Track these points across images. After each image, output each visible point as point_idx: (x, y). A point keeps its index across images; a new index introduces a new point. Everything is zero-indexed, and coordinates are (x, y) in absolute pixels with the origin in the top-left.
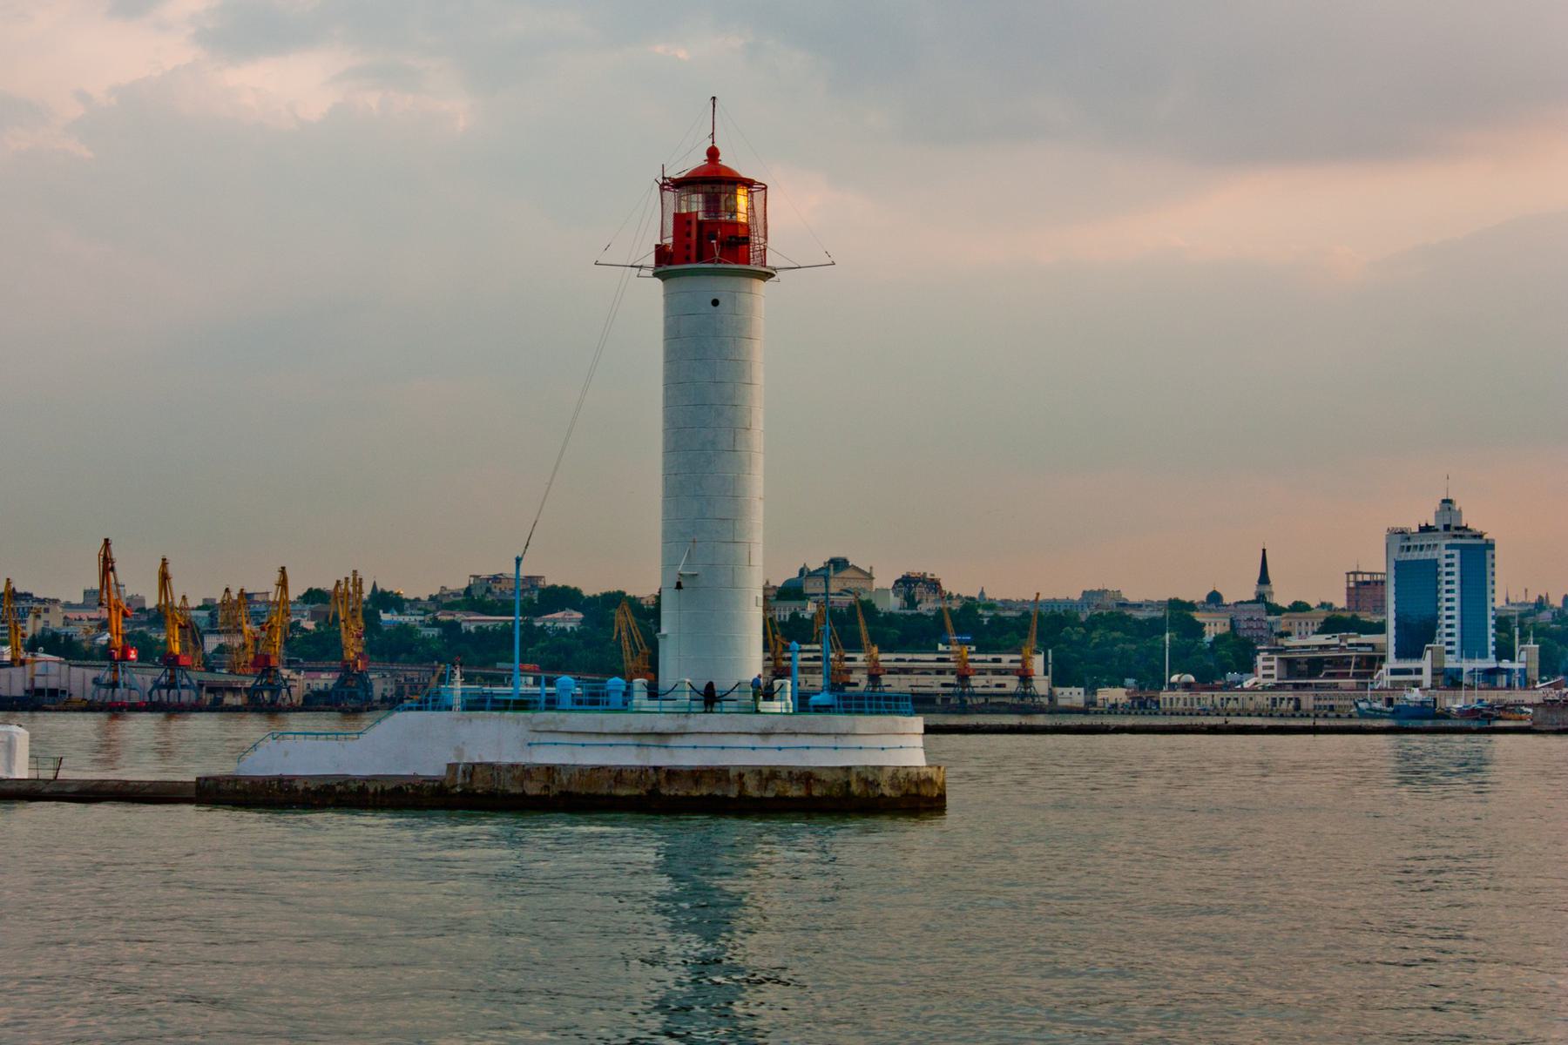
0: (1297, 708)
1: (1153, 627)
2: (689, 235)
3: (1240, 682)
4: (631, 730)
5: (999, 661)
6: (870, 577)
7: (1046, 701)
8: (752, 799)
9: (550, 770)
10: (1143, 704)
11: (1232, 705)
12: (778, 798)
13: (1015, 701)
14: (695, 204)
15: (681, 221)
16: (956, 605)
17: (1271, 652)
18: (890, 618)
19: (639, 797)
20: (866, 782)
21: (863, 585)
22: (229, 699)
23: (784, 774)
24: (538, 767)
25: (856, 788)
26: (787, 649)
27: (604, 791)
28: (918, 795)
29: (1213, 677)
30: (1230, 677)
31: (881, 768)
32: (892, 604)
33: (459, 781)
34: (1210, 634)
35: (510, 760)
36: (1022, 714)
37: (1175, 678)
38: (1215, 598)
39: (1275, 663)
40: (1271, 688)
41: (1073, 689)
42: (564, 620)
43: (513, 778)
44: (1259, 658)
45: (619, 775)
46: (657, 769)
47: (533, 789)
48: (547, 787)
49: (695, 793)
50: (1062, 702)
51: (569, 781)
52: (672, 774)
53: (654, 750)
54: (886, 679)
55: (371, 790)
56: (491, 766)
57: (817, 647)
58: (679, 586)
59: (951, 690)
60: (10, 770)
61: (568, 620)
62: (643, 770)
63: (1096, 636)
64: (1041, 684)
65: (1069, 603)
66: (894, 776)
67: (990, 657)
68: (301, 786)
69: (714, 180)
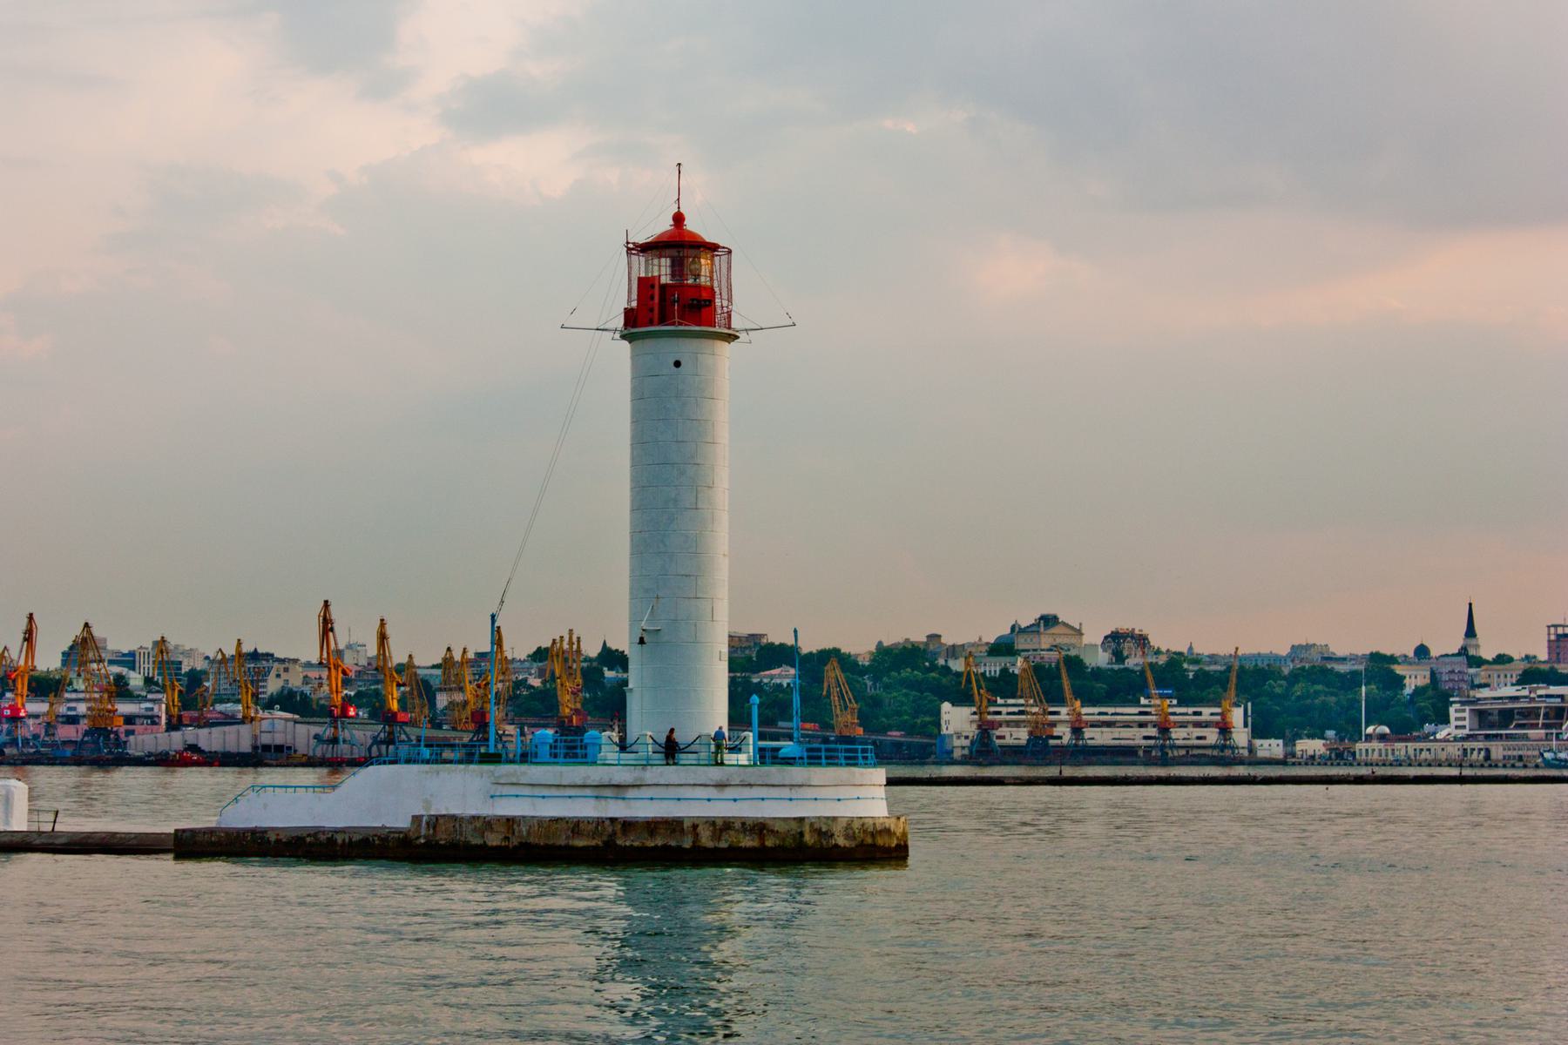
0: (1487, 758)
1: (1352, 680)
2: (652, 298)
3: (1434, 734)
4: (589, 782)
5: (1200, 714)
6: (1079, 633)
7: (1245, 753)
8: (706, 849)
9: (510, 821)
10: (1340, 755)
11: (1425, 755)
12: (731, 848)
13: (1215, 753)
14: (662, 270)
15: (646, 285)
16: (1162, 660)
17: (1462, 703)
18: (1097, 673)
19: (596, 847)
20: (819, 832)
21: (1073, 640)
22: (447, 754)
23: (738, 825)
24: (499, 819)
25: (809, 839)
26: (994, 703)
27: (562, 842)
28: (874, 845)
29: (1411, 730)
30: (1428, 727)
31: (834, 819)
32: (1101, 659)
33: (423, 832)
34: (1409, 687)
35: (473, 812)
36: (1223, 766)
37: (1370, 730)
38: (1422, 651)
39: (1466, 714)
40: (1463, 739)
41: (1273, 742)
42: (780, 676)
43: (475, 829)
44: (1452, 710)
45: (576, 826)
46: (613, 820)
47: (494, 840)
48: (506, 838)
49: (650, 844)
50: (1261, 754)
51: (529, 833)
52: (628, 825)
53: (611, 802)
54: (1088, 733)
55: (340, 841)
56: (454, 818)
57: (1022, 701)
58: (642, 641)
59: (1152, 742)
60: (7, 823)
61: (784, 676)
62: (600, 822)
63: (1298, 689)
64: (1241, 736)
65: (1277, 658)
66: (849, 826)
67: (1191, 710)
68: (273, 838)
69: (679, 245)
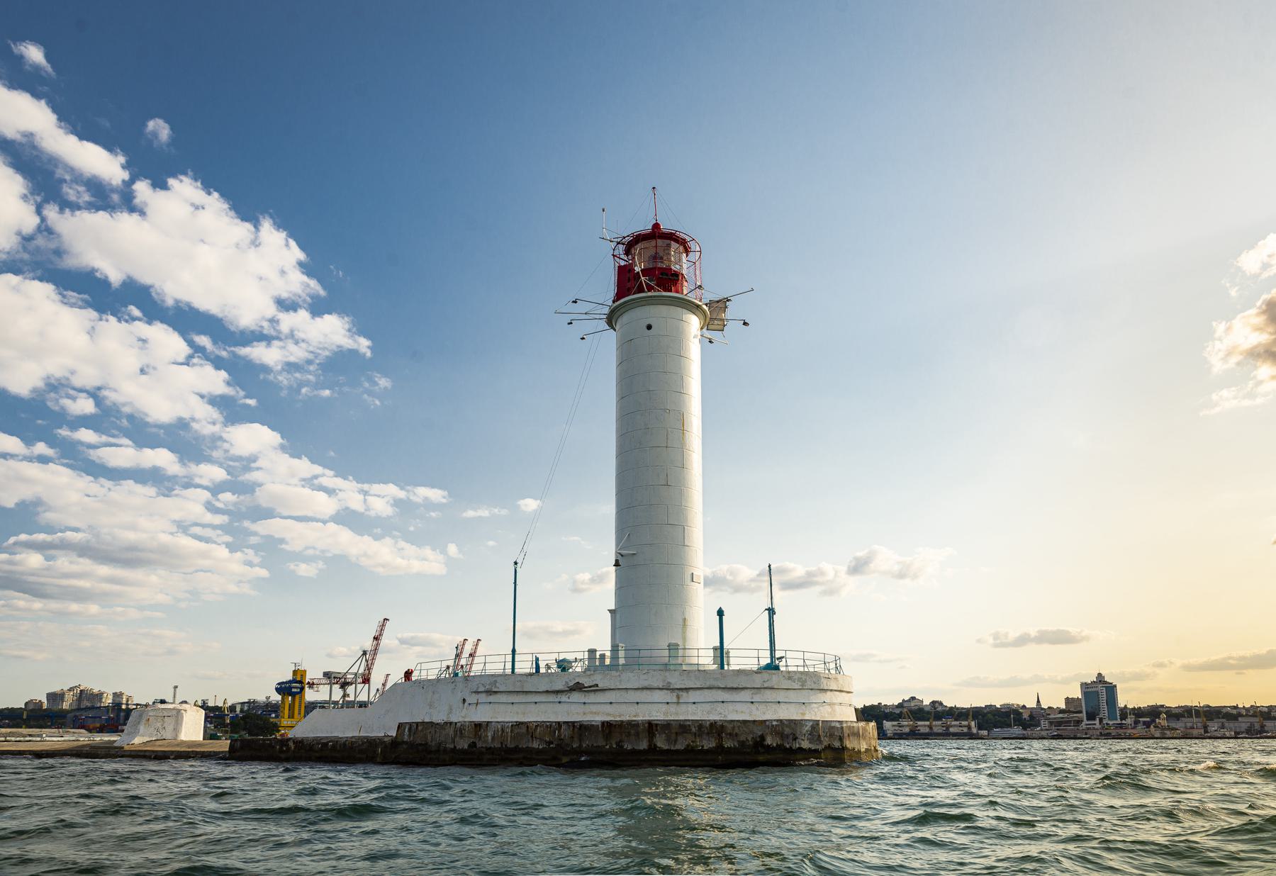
8: (663, 752)
9: (478, 726)
12: (690, 750)
20: (782, 736)
51: (493, 738)
